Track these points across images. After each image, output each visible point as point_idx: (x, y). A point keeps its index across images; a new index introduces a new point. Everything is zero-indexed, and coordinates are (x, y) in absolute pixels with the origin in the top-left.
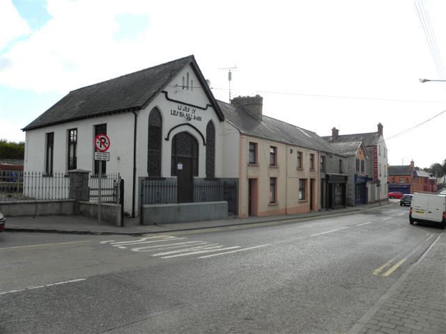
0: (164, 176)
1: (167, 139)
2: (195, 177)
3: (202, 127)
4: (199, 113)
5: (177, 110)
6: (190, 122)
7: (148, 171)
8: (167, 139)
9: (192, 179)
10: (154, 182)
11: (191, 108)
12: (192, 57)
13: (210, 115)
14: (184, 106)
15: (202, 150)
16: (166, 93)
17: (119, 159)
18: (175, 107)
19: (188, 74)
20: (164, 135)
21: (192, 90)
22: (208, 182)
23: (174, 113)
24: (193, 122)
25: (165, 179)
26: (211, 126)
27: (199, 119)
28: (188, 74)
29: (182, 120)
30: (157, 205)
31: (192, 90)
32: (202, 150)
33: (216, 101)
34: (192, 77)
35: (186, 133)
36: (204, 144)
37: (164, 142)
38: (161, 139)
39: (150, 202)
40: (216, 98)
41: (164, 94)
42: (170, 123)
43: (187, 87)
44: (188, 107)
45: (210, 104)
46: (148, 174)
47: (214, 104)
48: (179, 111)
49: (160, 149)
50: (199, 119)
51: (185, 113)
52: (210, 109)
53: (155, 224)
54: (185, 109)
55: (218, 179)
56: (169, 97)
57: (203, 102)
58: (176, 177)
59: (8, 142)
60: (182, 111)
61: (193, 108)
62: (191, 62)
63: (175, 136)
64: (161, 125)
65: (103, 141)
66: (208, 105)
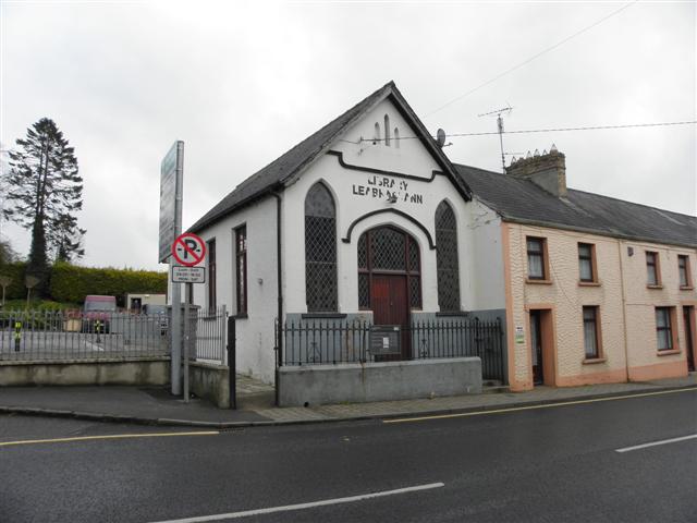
0: (342, 311)
1: (347, 241)
2: (415, 312)
3: (427, 215)
4: (414, 188)
5: (366, 185)
6: (395, 206)
7: (308, 303)
8: (347, 241)
9: (408, 316)
10: (317, 322)
11: (398, 180)
12: (392, 84)
13: (442, 190)
14: (380, 178)
15: (429, 260)
16: (339, 155)
17: (261, 283)
18: (362, 179)
19: (386, 117)
20: (341, 233)
21: (398, 146)
22: (446, 320)
23: (360, 191)
24: (399, 206)
25: (345, 316)
26: (446, 215)
27: (417, 199)
28: (386, 117)
29: (381, 203)
30: (314, 368)
31: (398, 146)
32: (429, 260)
33: (452, 165)
34: (396, 121)
35: (390, 227)
36: (432, 247)
37: (341, 247)
38: (334, 240)
39: (331, 359)
40: (452, 162)
41: (335, 159)
42: (354, 209)
43: (387, 139)
44: (390, 178)
45: (438, 169)
46: (306, 307)
47: (446, 169)
48: (371, 187)
49: (335, 260)
50: (417, 199)
51: (384, 189)
52: (441, 181)
53: (306, 405)
54: (385, 183)
55: (465, 315)
56: (346, 162)
57: (423, 165)
58: (371, 312)
59: (135, 269)
60: (377, 187)
61: (401, 180)
62: (392, 97)
63: (366, 234)
64: (335, 215)
65: (191, 245)
66: (435, 173)
